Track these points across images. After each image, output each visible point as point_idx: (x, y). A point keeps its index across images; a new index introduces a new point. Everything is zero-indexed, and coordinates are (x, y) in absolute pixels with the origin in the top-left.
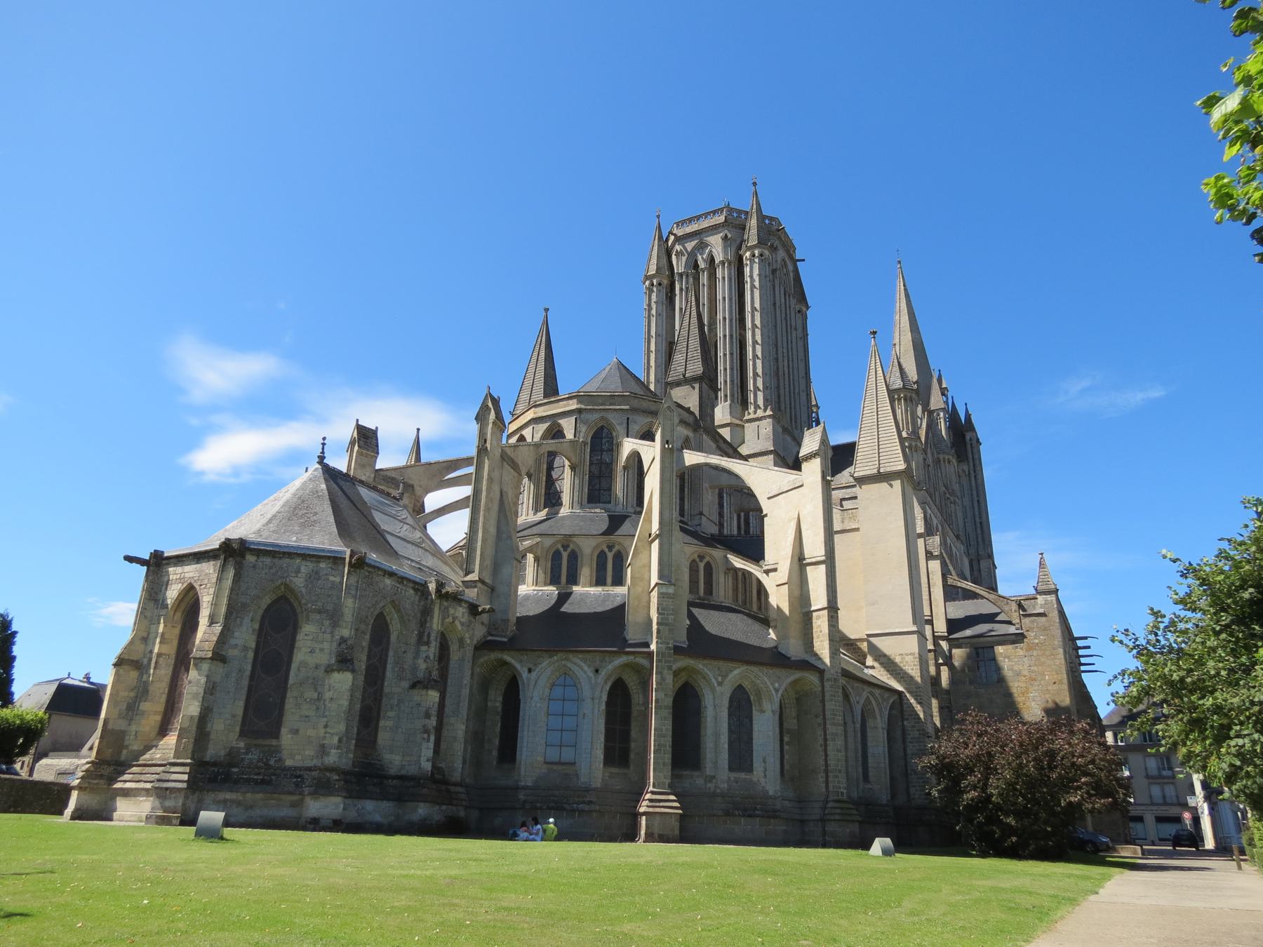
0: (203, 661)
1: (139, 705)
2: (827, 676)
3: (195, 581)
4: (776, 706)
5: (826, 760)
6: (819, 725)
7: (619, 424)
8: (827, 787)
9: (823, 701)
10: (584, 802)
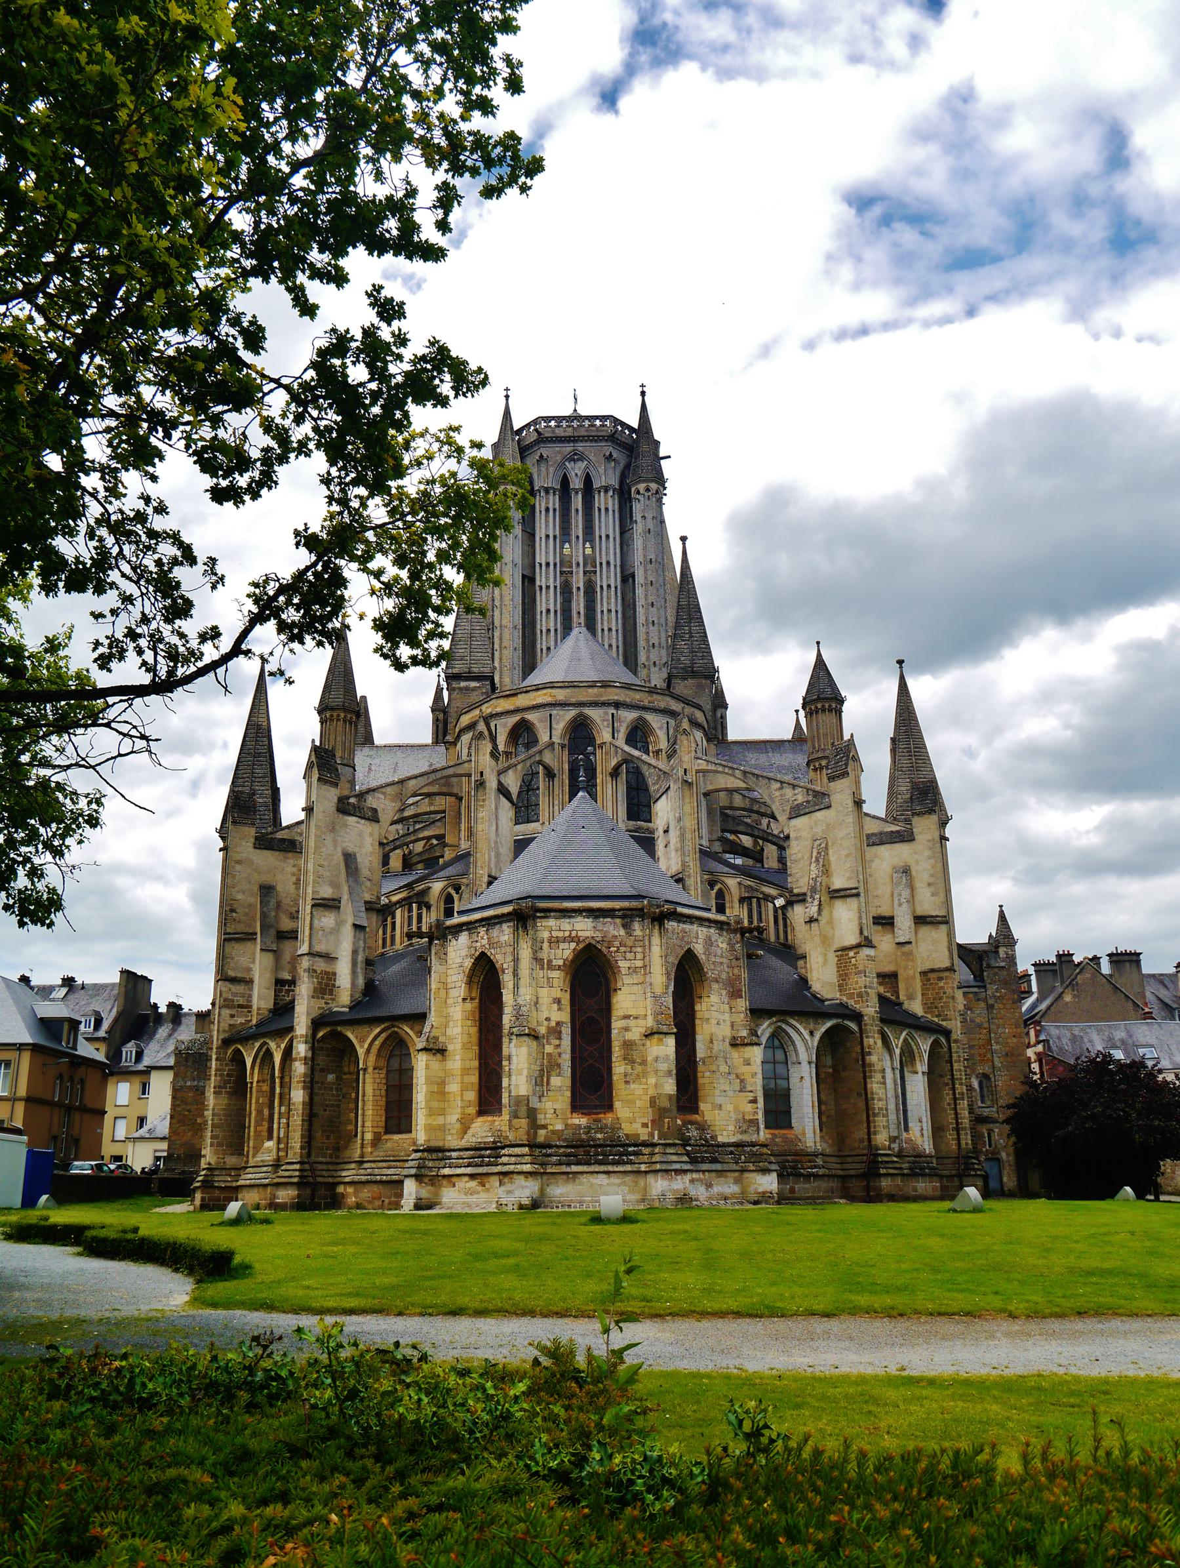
1: (548, 1080)
2: (954, 1036)
4: (925, 1069)
5: (957, 1119)
6: (947, 1084)
7: (661, 728)
8: (959, 1144)
9: (950, 1062)
10: (815, 1167)
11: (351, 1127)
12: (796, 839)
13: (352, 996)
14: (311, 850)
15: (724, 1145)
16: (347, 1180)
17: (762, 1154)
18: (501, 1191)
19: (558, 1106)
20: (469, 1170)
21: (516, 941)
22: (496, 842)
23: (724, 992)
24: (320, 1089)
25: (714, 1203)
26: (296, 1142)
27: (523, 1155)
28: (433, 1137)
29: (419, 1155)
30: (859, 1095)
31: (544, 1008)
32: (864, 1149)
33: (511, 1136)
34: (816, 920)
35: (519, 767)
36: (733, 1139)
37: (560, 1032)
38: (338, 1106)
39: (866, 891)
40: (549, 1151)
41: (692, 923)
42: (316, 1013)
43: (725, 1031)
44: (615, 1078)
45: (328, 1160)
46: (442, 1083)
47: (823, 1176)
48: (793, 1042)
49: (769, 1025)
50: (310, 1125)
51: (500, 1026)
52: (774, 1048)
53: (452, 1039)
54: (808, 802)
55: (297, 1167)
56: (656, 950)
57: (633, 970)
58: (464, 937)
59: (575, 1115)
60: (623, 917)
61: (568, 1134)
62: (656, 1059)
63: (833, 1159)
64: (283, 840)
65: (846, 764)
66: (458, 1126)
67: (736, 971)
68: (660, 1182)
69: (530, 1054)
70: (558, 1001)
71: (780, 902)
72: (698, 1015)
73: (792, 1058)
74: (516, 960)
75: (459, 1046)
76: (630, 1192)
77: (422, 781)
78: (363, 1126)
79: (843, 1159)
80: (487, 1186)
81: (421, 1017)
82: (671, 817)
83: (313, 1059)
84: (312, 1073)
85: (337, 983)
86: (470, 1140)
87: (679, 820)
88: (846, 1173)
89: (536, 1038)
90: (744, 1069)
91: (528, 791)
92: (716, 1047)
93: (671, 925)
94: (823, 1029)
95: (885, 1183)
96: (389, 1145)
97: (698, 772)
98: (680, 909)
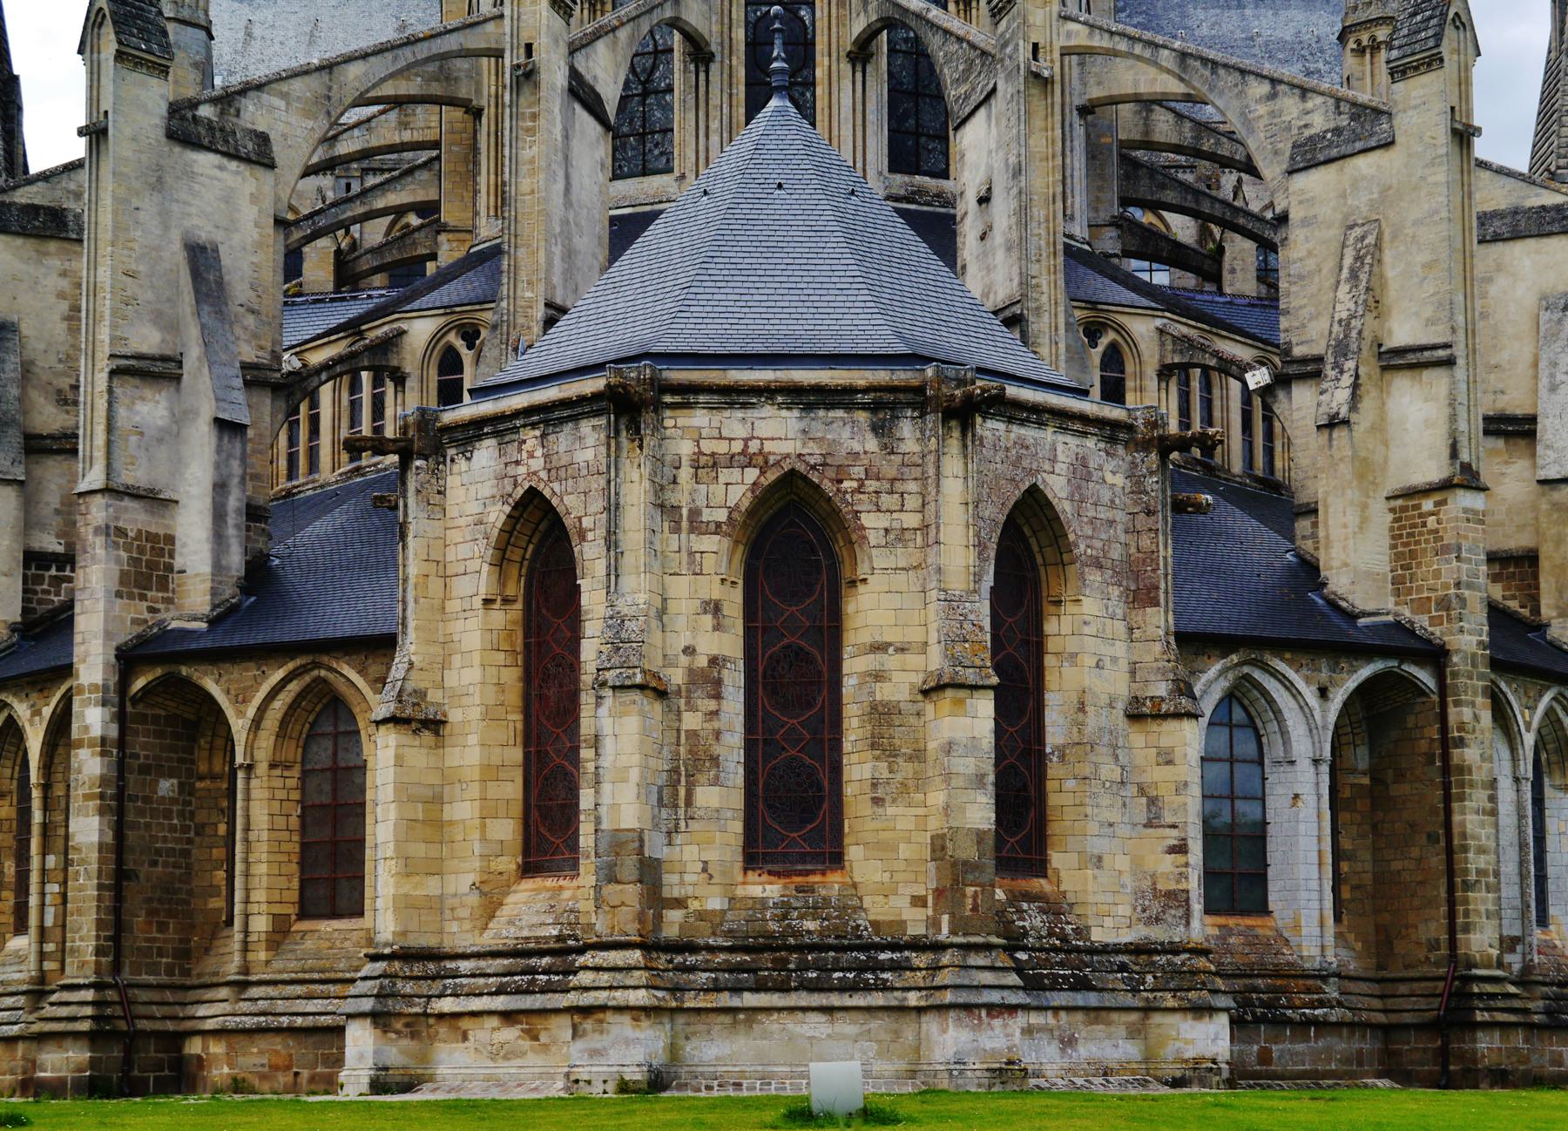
0: (976, 694)
3: (813, 467)
10: (1322, 1004)
11: (218, 903)
12: (1306, 222)
13: (214, 592)
14: (105, 235)
15: (1106, 949)
16: (210, 1025)
17: (1194, 972)
18: (576, 1051)
19: (711, 855)
20: (500, 1003)
21: (614, 462)
22: (565, 222)
23: (1115, 592)
24: (141, 813)
25: (1079, 1081)
26: (85, 937)
27: (629, 969)
28: (413, 926)
29: (380, 966)
30: (1432, 838)
31: (681, 624)
32: (1437, 964)
33: (602, 926)
34: (1346, 422)
35: (623, 34)
36: (1126, 937)
37: (718, 682)
38: (186, 854)
39: (1472, 352)
40: (691, 959)
41: (1041, 424)
42: (126, 634)
43: (1116, 685)
44: (849, 790)
45: (164, 979)
46: (437, 800)
47: (1339, 1025)
48: (1277, 713)
49: (1222, 673)
50: (119, 898)
51: (574, 666)
52: (1231, 726)
53: (458, 696)
54: (1337, 131)
55: (89, 995)
56: (953, 490)
57: (898, 536)
58: (486, 453)
59: (752, 876)
60: (874, 408)
61: (735, 920)
62: (949, 748)
63: (1364, 987)
64: (33, 210)
65: (1438, 37)
66: (474, 899)
67: (1146, 542)
68: (952, 1031)
69: (645, 733)
70: (714, 608)
71: (1258, 378)
72: (1052, 645)
73: (1274, 750)
74: (613, 509)
75: (475, 713)
76: (880, 1055)
77: (380, 66)
78: (247, 901)
79: (1389, 988)
80: (544, 1038)
81: (382, 645)
82: (998, 164)
83: (121, 743)
84: (121, 776)
85: (178, 562)
86: (501, 933)
87: (1017, 172)
88: (1394, 1018)
89: (662, 694)
90: (1159, 774)
91: (645, 94)
92: (1092, 721)
93: (990, 428)
94: (1352, 683)
95: (1486, 1045)
96: (309, 944)
97: (1066, 52)
98: (1012, 391)
